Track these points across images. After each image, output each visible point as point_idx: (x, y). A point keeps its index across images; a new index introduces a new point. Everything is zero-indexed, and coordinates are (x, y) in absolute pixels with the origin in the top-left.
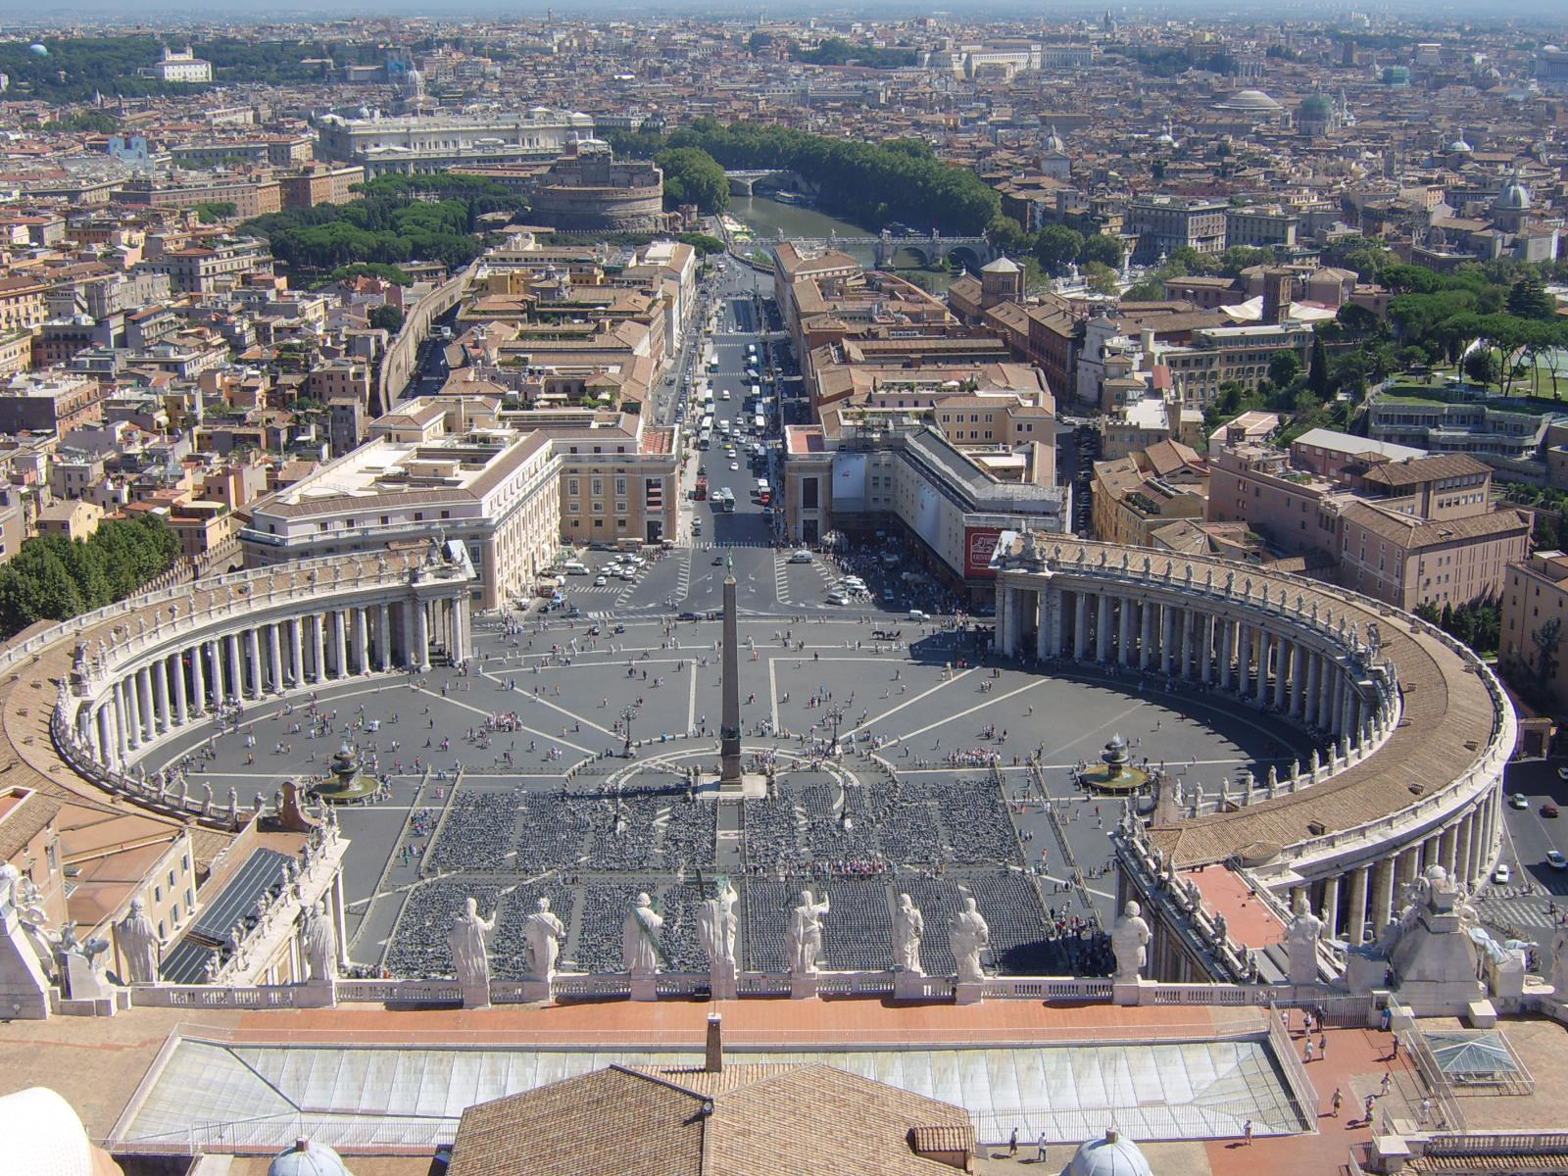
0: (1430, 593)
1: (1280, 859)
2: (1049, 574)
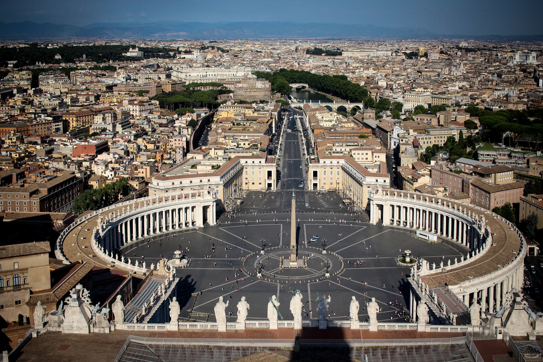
1: (458, 286)
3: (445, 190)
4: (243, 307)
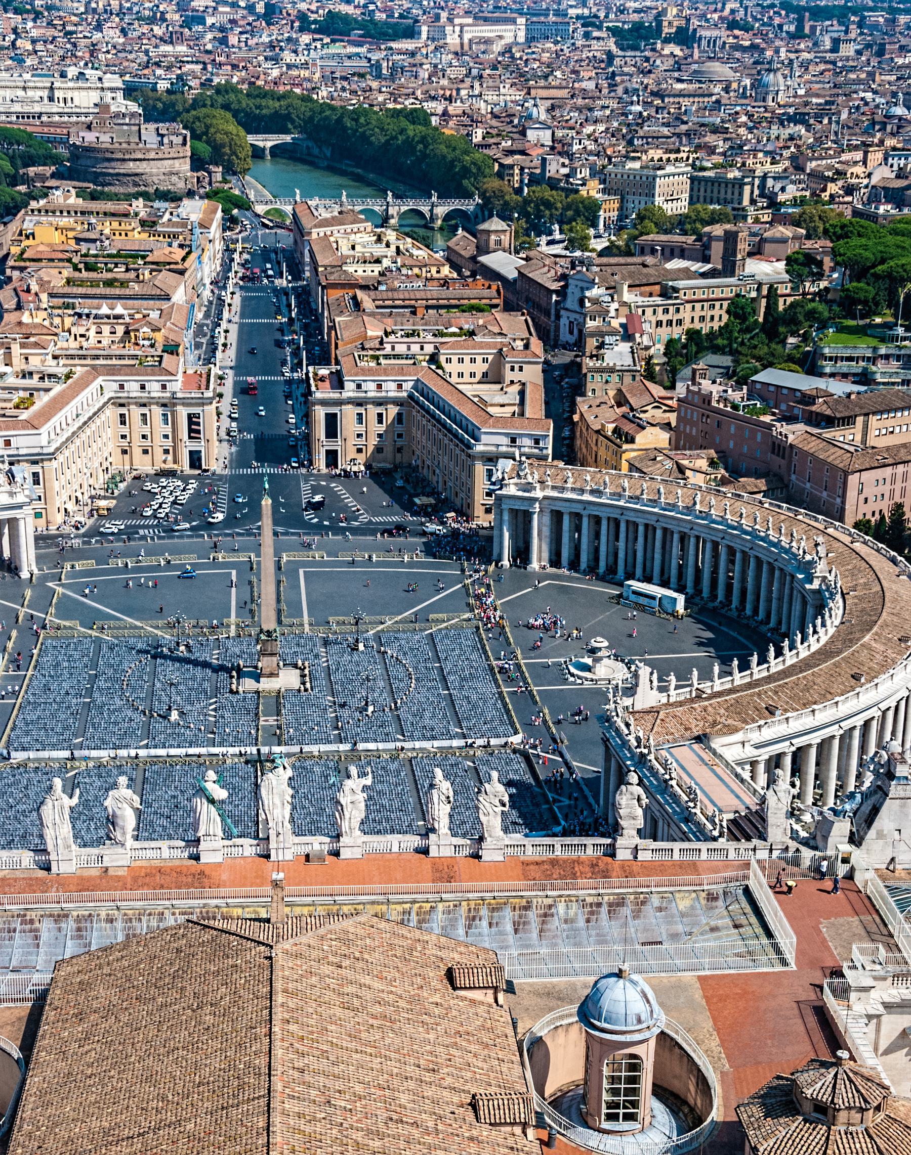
0: (867, 509)
2: (539, 494)
3: (712, 464)
4: (123, 802)
